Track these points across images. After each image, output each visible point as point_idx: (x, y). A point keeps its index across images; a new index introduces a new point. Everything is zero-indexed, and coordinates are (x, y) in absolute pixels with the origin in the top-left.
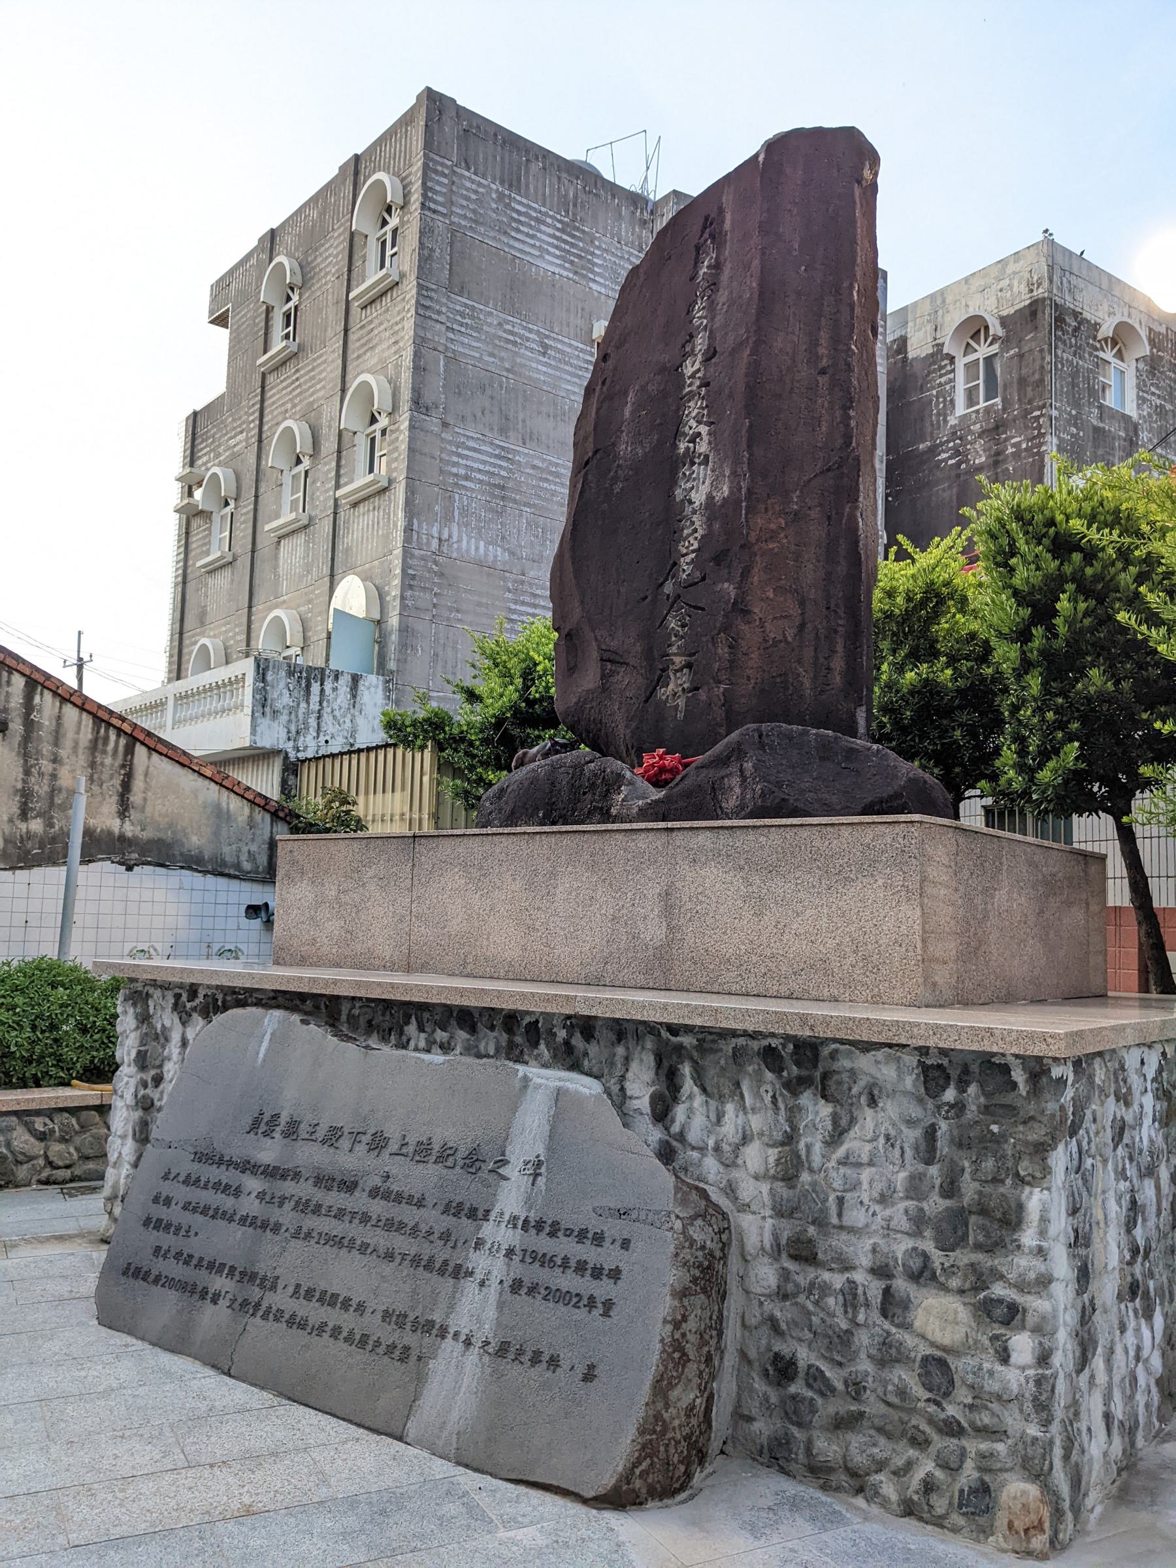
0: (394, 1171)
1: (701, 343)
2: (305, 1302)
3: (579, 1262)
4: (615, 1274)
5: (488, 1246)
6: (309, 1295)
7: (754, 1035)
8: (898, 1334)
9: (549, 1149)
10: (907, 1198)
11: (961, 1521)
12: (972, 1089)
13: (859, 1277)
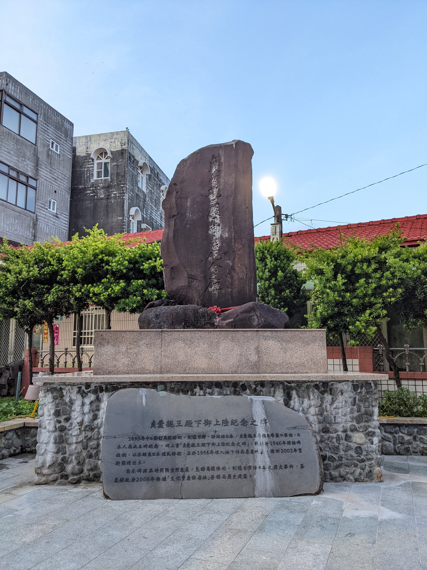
0: (217, 430)
1: (215, 191)
2: (202, 472)
3: (288, 442)
4: (299, 442)
5: (259, 443)
6: (203, 469)
7: (312, 382)
8: (350, 444)
9: (267, 416)
10: (350, 414)
11: (367, 479)
12: (364, 389)
13: (340, 433)
